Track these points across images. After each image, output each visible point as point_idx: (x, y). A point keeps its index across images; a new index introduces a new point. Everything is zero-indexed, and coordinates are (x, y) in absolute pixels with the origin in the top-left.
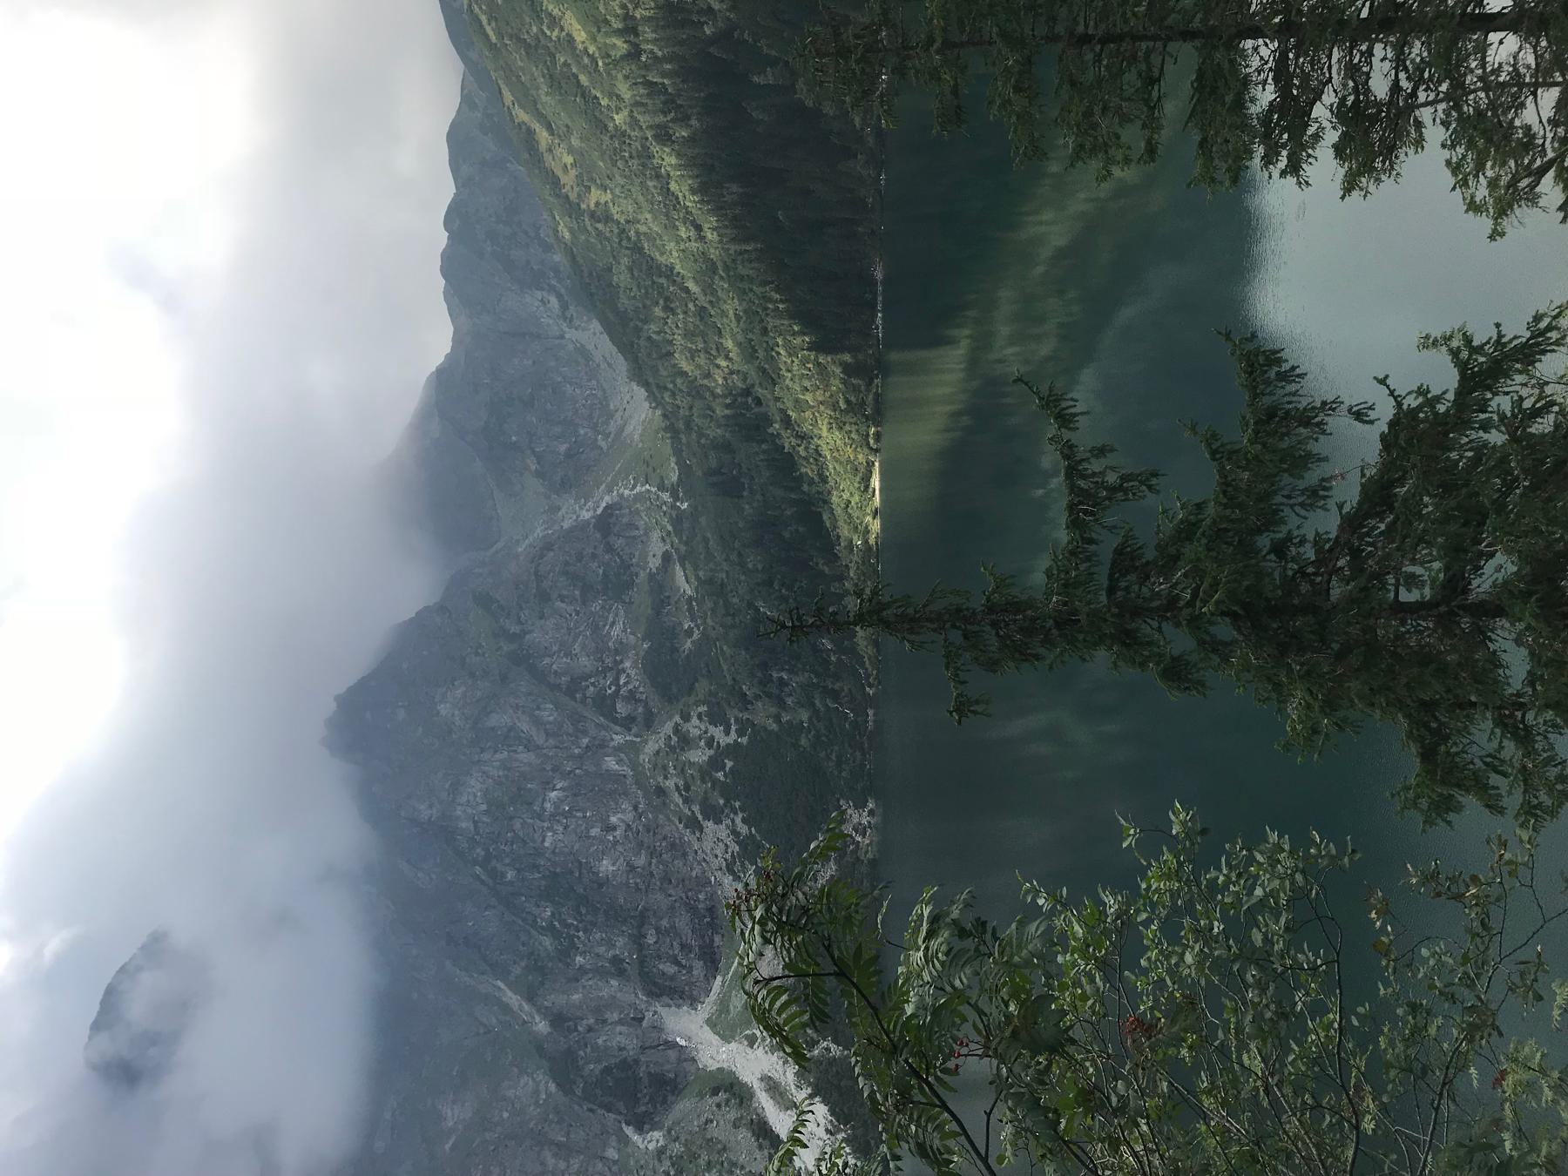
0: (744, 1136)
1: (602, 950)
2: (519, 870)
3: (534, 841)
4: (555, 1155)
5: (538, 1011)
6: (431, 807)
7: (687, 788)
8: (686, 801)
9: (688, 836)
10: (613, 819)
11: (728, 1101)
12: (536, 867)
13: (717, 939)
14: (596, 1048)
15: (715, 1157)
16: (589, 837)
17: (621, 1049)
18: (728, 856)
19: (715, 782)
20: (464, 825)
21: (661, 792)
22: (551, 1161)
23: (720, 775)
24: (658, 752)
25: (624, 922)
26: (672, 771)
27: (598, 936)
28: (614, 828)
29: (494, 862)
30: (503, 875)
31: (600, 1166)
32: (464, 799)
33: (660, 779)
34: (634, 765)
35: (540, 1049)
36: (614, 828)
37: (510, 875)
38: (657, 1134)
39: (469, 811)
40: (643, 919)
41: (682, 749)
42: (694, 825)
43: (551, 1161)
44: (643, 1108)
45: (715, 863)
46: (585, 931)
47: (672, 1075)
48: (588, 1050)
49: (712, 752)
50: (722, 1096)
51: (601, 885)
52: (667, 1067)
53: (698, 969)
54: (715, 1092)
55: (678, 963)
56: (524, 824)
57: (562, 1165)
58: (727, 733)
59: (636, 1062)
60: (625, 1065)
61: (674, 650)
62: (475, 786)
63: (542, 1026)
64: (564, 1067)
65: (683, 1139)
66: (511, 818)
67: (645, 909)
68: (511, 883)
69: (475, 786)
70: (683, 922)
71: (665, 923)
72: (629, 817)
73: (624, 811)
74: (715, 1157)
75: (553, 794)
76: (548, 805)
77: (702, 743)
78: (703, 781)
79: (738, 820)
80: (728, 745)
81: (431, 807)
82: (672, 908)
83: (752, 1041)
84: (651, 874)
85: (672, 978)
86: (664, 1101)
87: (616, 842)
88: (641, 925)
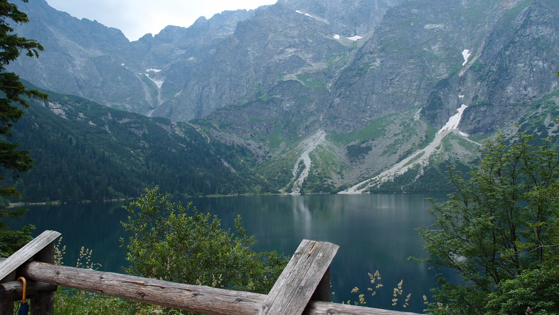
0: (409, 146)
1: (481, 91)
2: (509, 56)
3: (520, 60)
4: (417, 85)
5: (466, 71)
6: (536, 16)
7: (535, 117)
8: (531, 117)
9: (519, 119)
10: (529, 89)
11: (422, 141)
12: (510, 63)
13: (482, 133)
14: (448, 94)
15: (406, 137)
16: (521, 80)
17: (448, 102)
18: (506, 136)
19: (534, 128)
20: (528, 31)
21: (538, 106)
22: (415, 84)
23: (536, 130)
24: (554, 103)
25: (489, 99)
26: (545, 110)
27: (485, 89)
28: (525, 90)
29: (512, 46)
30: (507, 50)
31: (413, 100)
33: (543, 106)
34: (552, 95)
35: (453, 74)
36: (525, 90)
37: (507, 53)
38: (418, 118)
40: (489, 105)
41: (552, 114)
42: (523, 120)
43: (415, 84)
44: (426, 112)
45: (505, 131)
46: (487, 85)
47: (436, 121)
48: (447, 92)
49: (547, 126)
50: (424, 138)
51: (502, 88)
52: (439, 119)
53: (472, 127)
54: (426, 136)
55: (473, 119)
56: (527, 54)
57: (414, 88)
58: (553, 132)
59: (442, 108)
60: (441, 104)
62: (545, 31)
63: (461, 74)
64: (444, 83)
65: (415, 127)
66: (530, 49)
67: (493, 106)
68: (504, 54)
69: (545, 31)
70: (488, 120)
71: (487, 113)
72: (531, 95)
73: (533, 93)
74: (406, 137)
75: (541, 63)
76: (536, 62)
77: (552, 122)
78: (536, 123)
79: (514, 139)
80: (548, 133)
81: (536, 16)
82: (493, 116)
83: (438, 148)
84: (506, 106)
85: (469, 118)
86: (428, 119)
87: (519, 91)
88: (487, 104)
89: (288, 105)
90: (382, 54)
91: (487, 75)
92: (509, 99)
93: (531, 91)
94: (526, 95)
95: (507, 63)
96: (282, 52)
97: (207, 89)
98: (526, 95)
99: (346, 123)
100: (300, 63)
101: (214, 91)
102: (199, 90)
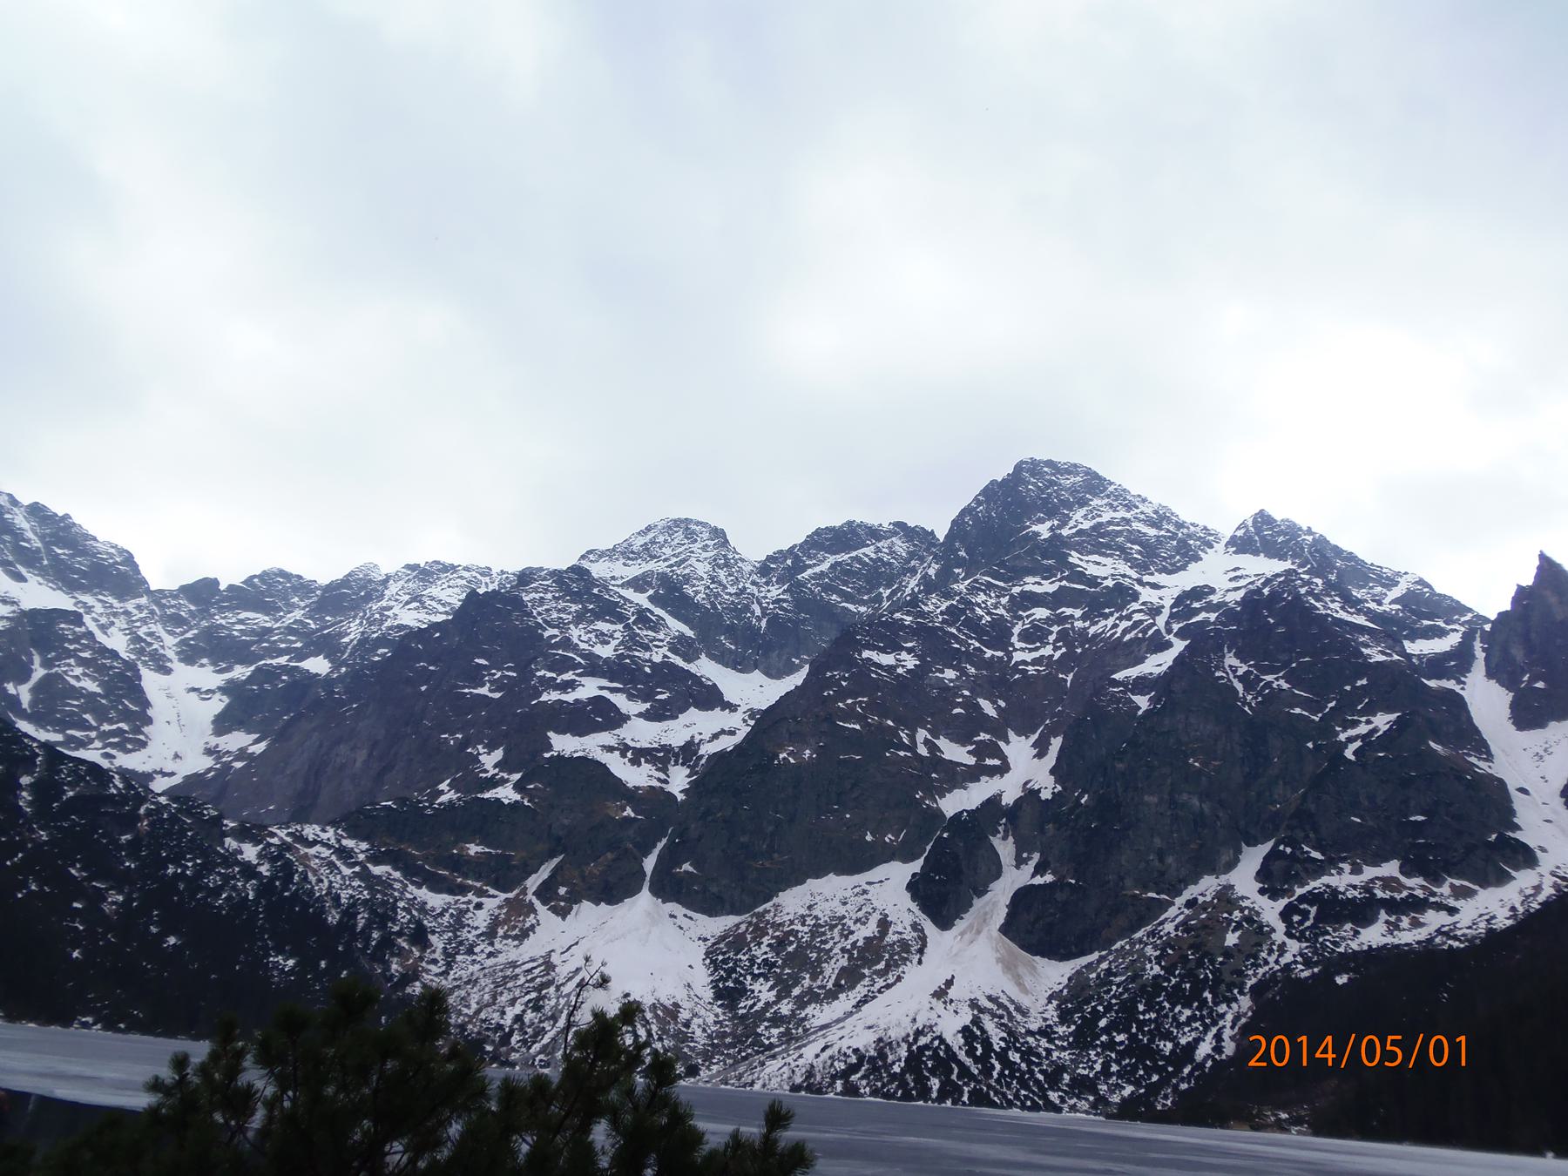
10: (1170, 860)
20: (1167, 721)
28: (1161, 860)
30: (1121, 760)
32: (1192, 720)
36: (1161, 860)
37: (1120, 766)
39: (1180, 726)
61: (1338, 920)
75: (1195, 802)
76: (1185, 797)
87: (1147, 862)
89: (566, 822)
90: (825, 727)
91: (1071, 811)
92: (1122, 879)
93: (1174, 865)
94: (1162, 874)
95: (1120, 791)
96: (570, 686)
97: (343, 749)
98: (1162, 874)
99: (714, 889)
100: (615, 719)
101: (362, 755)
102: (321, 746)
